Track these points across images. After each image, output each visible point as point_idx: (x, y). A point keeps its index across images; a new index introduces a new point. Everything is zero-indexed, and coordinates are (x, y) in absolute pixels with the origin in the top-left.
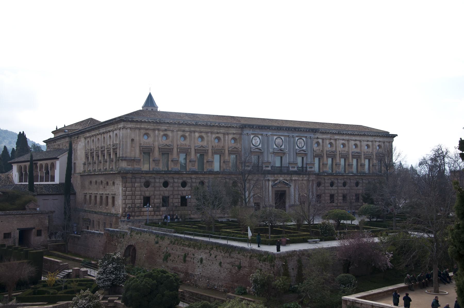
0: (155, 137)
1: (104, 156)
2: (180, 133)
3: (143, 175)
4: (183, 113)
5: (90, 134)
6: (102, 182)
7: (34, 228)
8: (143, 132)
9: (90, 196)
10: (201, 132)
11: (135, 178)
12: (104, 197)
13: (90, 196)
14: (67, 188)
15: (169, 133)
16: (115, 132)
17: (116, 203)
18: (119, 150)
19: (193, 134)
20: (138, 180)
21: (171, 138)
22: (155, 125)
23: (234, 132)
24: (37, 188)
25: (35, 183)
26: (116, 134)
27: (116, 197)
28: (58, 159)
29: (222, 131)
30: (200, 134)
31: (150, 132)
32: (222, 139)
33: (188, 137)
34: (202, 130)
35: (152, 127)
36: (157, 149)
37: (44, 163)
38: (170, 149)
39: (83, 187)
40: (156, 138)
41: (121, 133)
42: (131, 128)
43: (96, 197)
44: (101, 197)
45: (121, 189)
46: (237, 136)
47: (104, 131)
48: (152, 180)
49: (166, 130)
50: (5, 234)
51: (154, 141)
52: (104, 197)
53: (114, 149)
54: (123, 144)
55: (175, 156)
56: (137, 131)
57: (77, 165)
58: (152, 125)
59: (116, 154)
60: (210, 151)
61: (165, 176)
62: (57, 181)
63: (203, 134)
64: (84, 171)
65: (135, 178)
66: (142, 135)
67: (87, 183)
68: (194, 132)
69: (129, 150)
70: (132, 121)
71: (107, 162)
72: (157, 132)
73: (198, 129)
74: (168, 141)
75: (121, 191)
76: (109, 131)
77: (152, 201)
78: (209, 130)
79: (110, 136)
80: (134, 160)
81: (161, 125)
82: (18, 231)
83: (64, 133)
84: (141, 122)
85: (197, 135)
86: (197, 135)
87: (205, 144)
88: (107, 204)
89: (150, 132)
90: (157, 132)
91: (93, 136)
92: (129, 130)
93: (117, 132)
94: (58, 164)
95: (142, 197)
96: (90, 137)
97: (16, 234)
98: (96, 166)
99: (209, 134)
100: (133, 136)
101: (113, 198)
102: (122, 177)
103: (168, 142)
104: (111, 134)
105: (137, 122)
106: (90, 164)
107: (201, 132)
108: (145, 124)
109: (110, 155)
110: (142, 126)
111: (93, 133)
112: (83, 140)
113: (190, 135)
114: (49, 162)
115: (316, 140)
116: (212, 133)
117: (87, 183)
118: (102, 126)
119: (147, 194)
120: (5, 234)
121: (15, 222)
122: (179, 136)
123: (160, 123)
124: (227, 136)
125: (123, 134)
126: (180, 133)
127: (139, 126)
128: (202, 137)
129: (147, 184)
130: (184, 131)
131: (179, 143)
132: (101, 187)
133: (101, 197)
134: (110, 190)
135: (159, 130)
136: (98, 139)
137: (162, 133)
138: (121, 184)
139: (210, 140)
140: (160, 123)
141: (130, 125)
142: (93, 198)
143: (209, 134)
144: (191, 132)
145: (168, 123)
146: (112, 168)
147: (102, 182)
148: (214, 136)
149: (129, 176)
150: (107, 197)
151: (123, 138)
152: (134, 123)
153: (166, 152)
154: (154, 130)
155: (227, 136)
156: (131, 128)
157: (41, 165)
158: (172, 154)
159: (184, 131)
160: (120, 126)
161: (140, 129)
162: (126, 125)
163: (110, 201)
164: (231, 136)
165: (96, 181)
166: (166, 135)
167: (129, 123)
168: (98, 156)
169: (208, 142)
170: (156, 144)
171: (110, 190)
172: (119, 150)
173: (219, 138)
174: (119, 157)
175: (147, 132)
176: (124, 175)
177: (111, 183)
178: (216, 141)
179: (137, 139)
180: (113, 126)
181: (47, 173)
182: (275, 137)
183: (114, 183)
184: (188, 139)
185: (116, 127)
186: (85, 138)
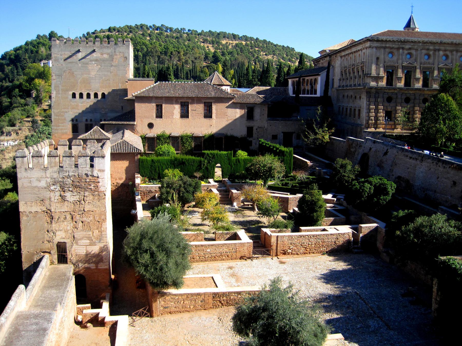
1: (354, 72)
2: (424, 52)
3: (385, 91)
4: (429, 33)
5: (345, 54)
6: (352, 96)
7: (295, 133)
8: (388, 50)
9: (343, 108)
10: (445, 50)
12: (353, 109)
13: (343, 108)
14: (325, 100)
15: (413, 52)
16: (363, 51)
17: (361, 115)
18: (366, 67)
19: (437, 53)
20: (381, 95)
21: (414, 57)
22: (400, 43)
25: (300, 95)
26: (364, 53)
27: (361, 110)
28: (320, 75)
30: (445, 53)
34: (448, 48)
35: (397, 46)
38: (413, 67)
40: (400, 57)
41: (368, 51)
42: (376, 48)
43: (347, 109)
44: (351, 109)
45: (365, 102)
47: (355, 50)
48: (394, 96)
49: (410, 49)
50: (273, 136)
51: (398, 60)
52: (353, 109)
53: (362, 67)
54: (368, 62)
56: (382, 50)
57: (335, 80)
58: (397, 43)
59: (363, 71)
61: (406, 92)
62: (318, 95)
63: (448, 53)
64: (339, 86)
66: (386, 53)
67: (341, 97)
68: (439, 50)
71: (356, 78)
72: (401, 50)
73: (442, 48)
74: (412, 59)
76: (359, 51)
78: (454, 48)
79: (359, 55)
81: (406, 44)
83: (325, 53)
84: (386, 41)
85: (441, 53)
88: (354, 117)
89: (395, 51)
90: (401, 50)
91: (347, 55)
92: (374, 49)
94: (319, 78)
96: (345, 56)
97: (281, 136)
99: (454, 53)
100: (378, 55)
101: (359, 110)
102: (367, 92)
104: (360, 52)
105: (382, 41)
106: (344, 79)
107: (445, 50)
108: (390, 43)
110: (387, 45)
111: (347, 52)
112: (339, 58)
114: (313, 78)
117: (341, 97)
118: (353, 46)
119: (389, 110)
120: (273, 136)
121: (280, 127)
122: (423, 54)
125: (369, 53)
126: (424, 52)
127: (384, 45)
128: (447, 57)
130: (428, 49)
131: (423, 61)
133: (351, 109)
135: (403, 48)
136: (351, 58)
137: (406, 52)
138: (365, 98)
139: (455, 58)
141: (376, 44)
142: (345, 109)
144: (435, 50)
145: (412, 42)
146: (360, 84)
147: (352, 96)
151: (369, 57)
152: (380, 43)
154: (398, 49)
156: (376, 48)
159: (428, 49)
160: (367, 46)
161: (385, 48)
162: (372, 45)
166: (410, 54)
167: (375, 42)
168: (350, 73)
172: (366, 67)
174: (365, 74)
175: (392, 50)
177: (358, 97)
179: (382, 57)
180: (361, 45)
181: (312, 87)
183: (360, 97)
185: (364, 47)
186: (341, 57)
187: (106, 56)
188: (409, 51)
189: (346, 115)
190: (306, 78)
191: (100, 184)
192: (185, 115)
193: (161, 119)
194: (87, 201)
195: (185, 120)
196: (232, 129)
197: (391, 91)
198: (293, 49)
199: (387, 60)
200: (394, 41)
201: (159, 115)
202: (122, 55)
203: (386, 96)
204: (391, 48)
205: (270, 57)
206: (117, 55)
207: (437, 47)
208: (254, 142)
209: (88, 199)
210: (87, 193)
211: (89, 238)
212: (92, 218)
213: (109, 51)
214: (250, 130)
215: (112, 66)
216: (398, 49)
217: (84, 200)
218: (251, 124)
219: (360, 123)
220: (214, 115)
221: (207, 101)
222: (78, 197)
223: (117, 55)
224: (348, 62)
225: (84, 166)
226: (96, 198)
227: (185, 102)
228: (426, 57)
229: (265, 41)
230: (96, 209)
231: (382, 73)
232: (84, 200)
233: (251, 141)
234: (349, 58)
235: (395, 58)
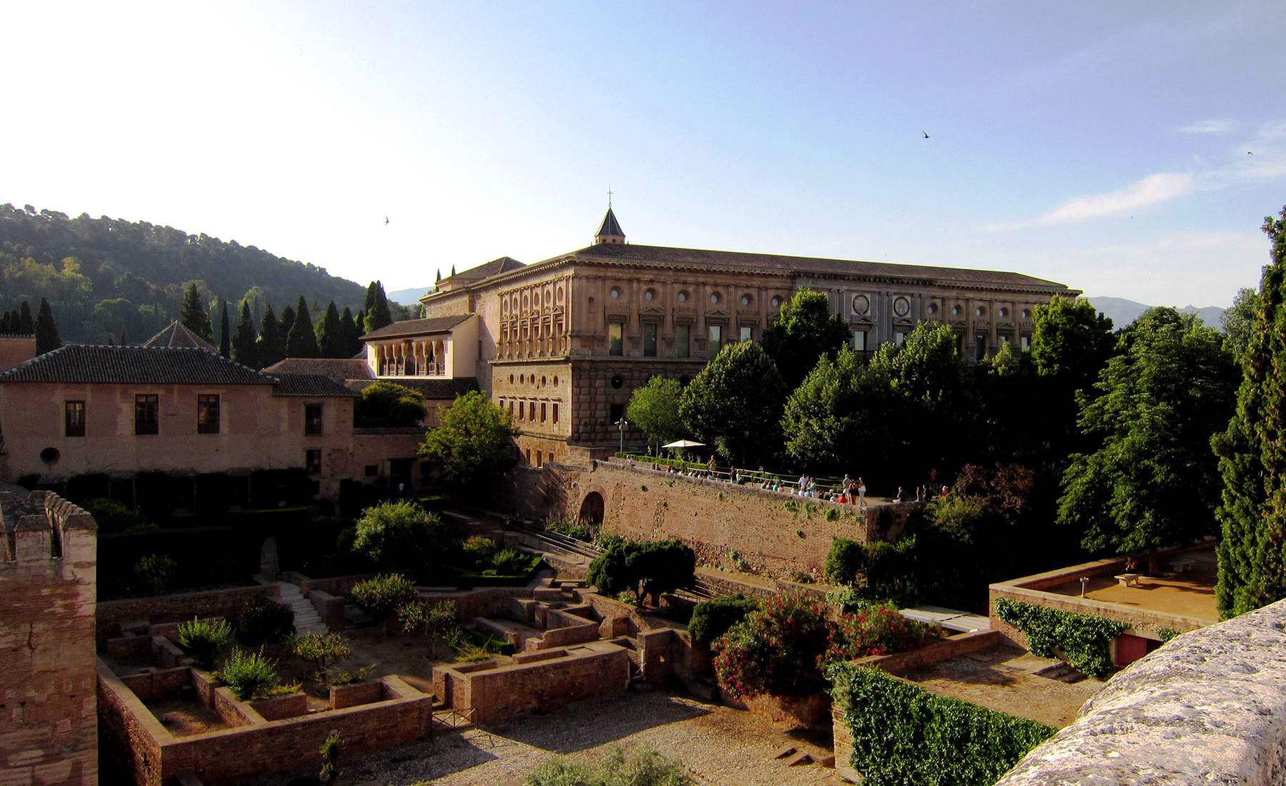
0: (632, 293)
2: (678, 287)
6: (533, 377)
8: (609, 284)
10: (716, 285)
11: (596, 370)
12: (538, 404)
15: (658, 287)
17: (561, 415)
19: (701, 289)
20: (601, 374)
23: (779, 285)
29: (756, 282)
31: (624, 286)
33: (693, 295)
34: (719, 281)
36: (635, 317)
42: (587, 278)
46: (783, 293)
49: (651, 281)
51: (630, 302)
52: (538, 404)
55: (668, 329)
56: (600, 283)
60: (733, 321)
62: (448, 374)
63: (720, 289)
65: (596, 370)
68: (704, 284)
69: (584, 319)
70: (591, 265)
72: (635, 285)
73: (710, 279)
80: (594, 337)
84: (607, 265)
85: (709, 290)
86: (709, 290)
87: (723, 307)
88: (543, 418)
89: (624, 286)
90: (635, 285)
92: (584, 282)
95: (608, 407)
99: (732, 289)
100: (592, 292)
101: (556, 406)
103: (656, 304)
105: (600, 265)
113: (696, 291)
119: (618, 400)
124: (764, 294)
126: (678, 287)
127: (602, 274)
128: (718, 295)
130: (685, 283)
131: (676, 305)
132: (534, 387)
135: (638, 280)
137: (644, 287)
142: (517, 406)
143: (732, 289)
144: (697, 284)
147: (533, 377)
148: (740, 292)
154: (630, 280)
155: (764, 294)
159: (685, 283)
161: (604, 279)
163: (550, 412)
164: (772, 293)
165: (522, 377)
166: (652, 291)
169: (729, 302)
170: (634, 306)
171: (550, 392)
173: (749, 297)
175: (618, 284)
178: (745, 301)
179: (599, 297)
181: (431, 358)
183: (556, 380)
184: (693, 298)
186: (501, 296)
189: (522, 416)
191: (81, 598)
193: (82, 438)
194: (41, 647)
195: (146, 439)
197: (619, 366)
198: (323, 271)
199: (608, 304)
201: (75, 429)
203: (610, 375)
204: (617, 280)
207: (701, 279)
208: (323, 484)
209: (43, 639)
210: (39, 627)
211: (41, 744)
212: (51, 690)
214: (312, 455)
216: (630, 280)
217: (29, 645)
218: (315, 443)
220: (224, 426)
221: (206, 392)
222: (11, 638)
225: (34, 557)
226: (68, 635)
227: (147, 396)
228: (682, 297)
229: (252, 250)
230: (65, 664)
232: (29, 645)
233: (318, 483)
235: (625, 299)
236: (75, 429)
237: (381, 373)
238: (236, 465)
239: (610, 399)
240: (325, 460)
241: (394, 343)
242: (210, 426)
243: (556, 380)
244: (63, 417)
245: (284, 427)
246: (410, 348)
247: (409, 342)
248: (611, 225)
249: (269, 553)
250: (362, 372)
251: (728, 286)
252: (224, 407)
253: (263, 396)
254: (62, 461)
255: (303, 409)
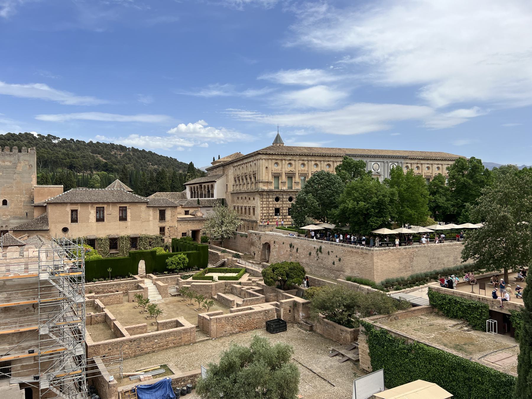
0: (282, 165)
2: (301, 162)
8: (274, 161)
10: (316, 161)
12: (247, 208)
15: (293, 162)
16: (254, 162)
19: (310, 162)
20: (271, 196)
21: (294, 166)
24: (202, 202)
29: (332, 159)
30: (316, 162)
31: (279, 162)
32: (332, 165)
34: (317, 159)
37: (206, 184)
39: (233, 201)
44: (245, 208)
45: (259, 202)
49: (290, 160)
51: (282, 168)
53: (254, 174)
56: (270, 161)
62: (215, 197)
63: (318, 162)
64: (234, 190)
66: (273, 164)
68: (311, 161)
70: (266, 154)
73: (313, 159)
75: (259, 204)
77: (281, 211)
82: (191, 232)
84: (272, 154)
86: (313, 163)
89: (279, 162)
92: (264, 161)
93: (256, 162)
94: (216, 185)
95: (274, 209)
97: (190, 234)
98: (241, 186)
99: (322, 162)
101: (254, 209)
104: (252, 163)
105: (270, 154)
109: (251, 178)
111: (239, 163)
112: (232, 168)
114: (210, 184)
115: (406, 165)
116: (324, 161)
117: (236, 198)
119: (278, 206)
123: (286, 155)
129: (277, 199)
130: (303, 160)
131: (300, 170)
133: (245, 208)
134: (251, 203)
137: (287, 162)
140: (286, 155)
142: (240, 208)
143: (322, 162)
148: (326, 163)
149: (265, 193)
150: (250, 209)
153: (290, 176)
154: (282, 160)
157: (205, 186)
158: (295, 177)
159: (303, 160)
161: (272, 159)
163: (252, 211)
166: (290, 164)
170: (284, 170)
171: (251, 203)
176: (261, 193)
177: (252, 199)
181: (209, 192)
182: (373, 163)
183: (254, 199)
184: (307, 166)
187: (8, 164)
188: (290, 162)
190: (203, 185)
192: (100, 219)
195: (100, 223)
196: (146, 230)
198: (176, 160)
199: (273, 169)
200: (278, 154)
201: (74, 220)
202: (27, 163)
205: (156, 167)
206: (20, 163)
213: (12, 159)
214: (162, 230)
215: (15, 173)
216: (282, 160)
219: (255, 219)
220: (129, 218)
223: (20, 163)
224: (240, 171)
231: (271, 179)
234: (241, 168)
236: (74, 220)
237: (192, 197)
238: (133, 233)
239: (274, 206)
240: (166, 230)
241: (196, 185)
242: (123, 218)
243: (254, 199)
244: (70, 216)
245: (151, 218)
246: (201, 188)
247: (201, 186)
248: (278, 139)
249: (142, 265)
250: (184, 197)
251: (321, 161)
252: (129, 211)
253: (143, 207)
254: (69, 232)
255: (158, 212)
